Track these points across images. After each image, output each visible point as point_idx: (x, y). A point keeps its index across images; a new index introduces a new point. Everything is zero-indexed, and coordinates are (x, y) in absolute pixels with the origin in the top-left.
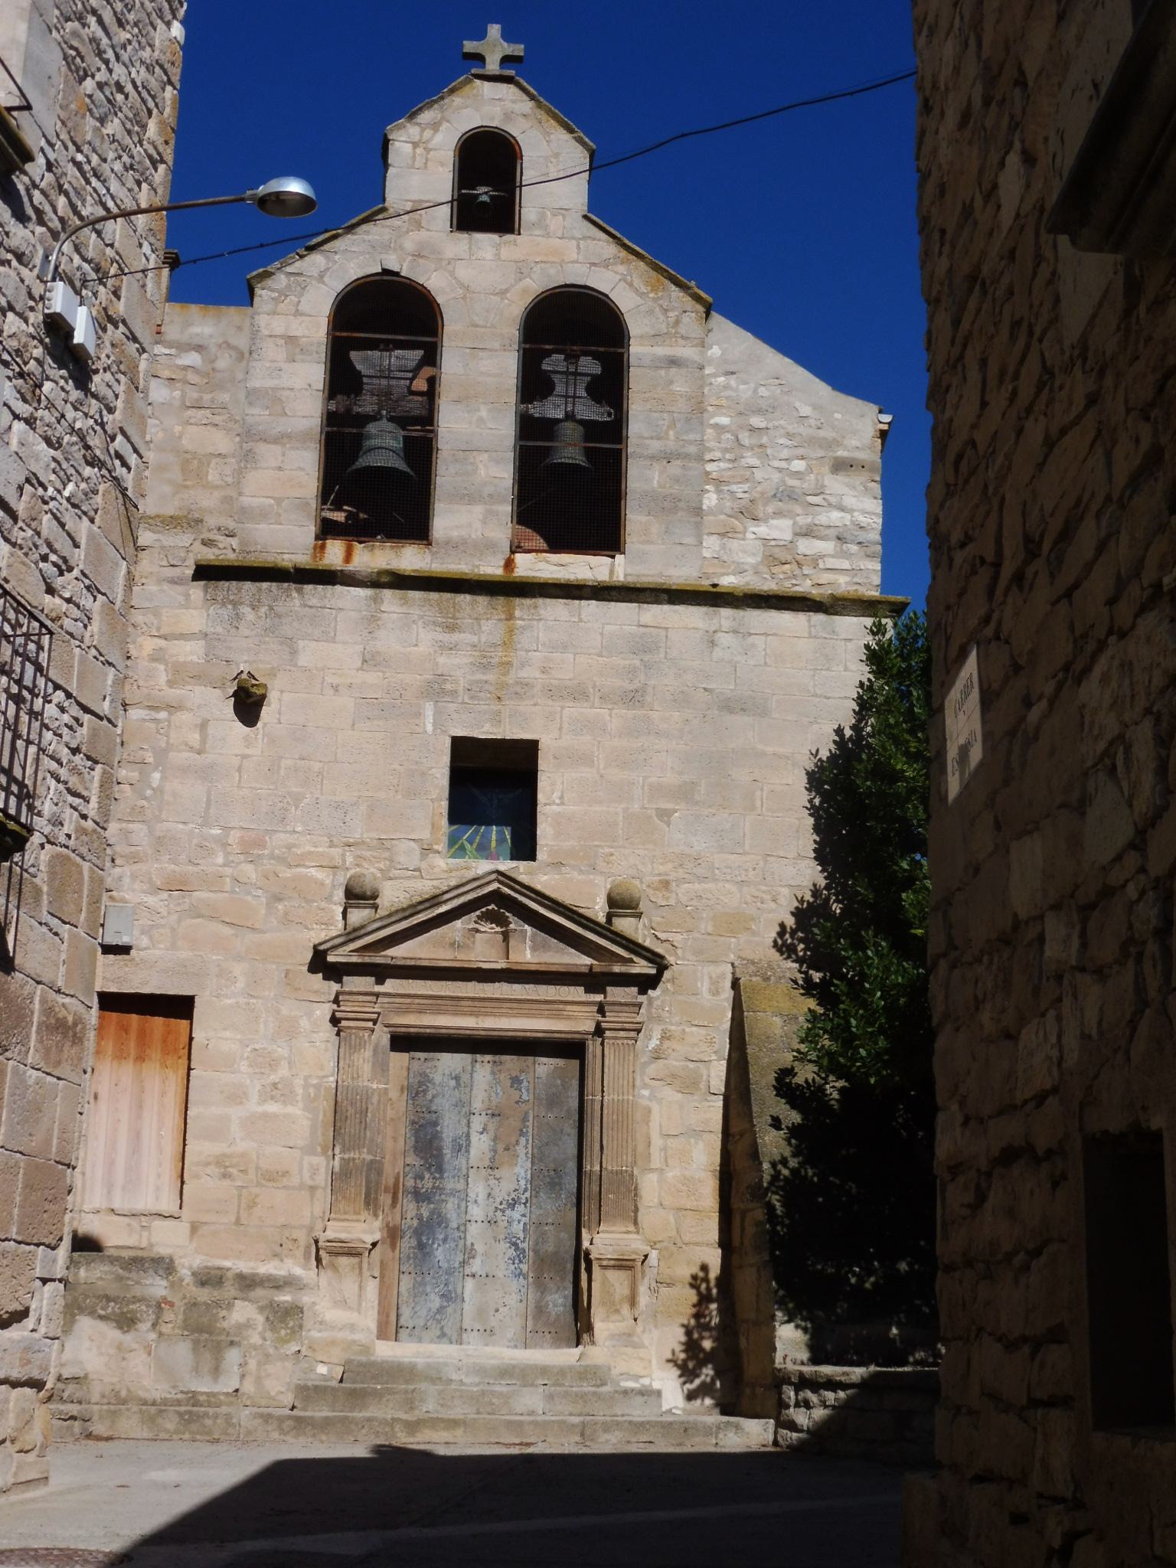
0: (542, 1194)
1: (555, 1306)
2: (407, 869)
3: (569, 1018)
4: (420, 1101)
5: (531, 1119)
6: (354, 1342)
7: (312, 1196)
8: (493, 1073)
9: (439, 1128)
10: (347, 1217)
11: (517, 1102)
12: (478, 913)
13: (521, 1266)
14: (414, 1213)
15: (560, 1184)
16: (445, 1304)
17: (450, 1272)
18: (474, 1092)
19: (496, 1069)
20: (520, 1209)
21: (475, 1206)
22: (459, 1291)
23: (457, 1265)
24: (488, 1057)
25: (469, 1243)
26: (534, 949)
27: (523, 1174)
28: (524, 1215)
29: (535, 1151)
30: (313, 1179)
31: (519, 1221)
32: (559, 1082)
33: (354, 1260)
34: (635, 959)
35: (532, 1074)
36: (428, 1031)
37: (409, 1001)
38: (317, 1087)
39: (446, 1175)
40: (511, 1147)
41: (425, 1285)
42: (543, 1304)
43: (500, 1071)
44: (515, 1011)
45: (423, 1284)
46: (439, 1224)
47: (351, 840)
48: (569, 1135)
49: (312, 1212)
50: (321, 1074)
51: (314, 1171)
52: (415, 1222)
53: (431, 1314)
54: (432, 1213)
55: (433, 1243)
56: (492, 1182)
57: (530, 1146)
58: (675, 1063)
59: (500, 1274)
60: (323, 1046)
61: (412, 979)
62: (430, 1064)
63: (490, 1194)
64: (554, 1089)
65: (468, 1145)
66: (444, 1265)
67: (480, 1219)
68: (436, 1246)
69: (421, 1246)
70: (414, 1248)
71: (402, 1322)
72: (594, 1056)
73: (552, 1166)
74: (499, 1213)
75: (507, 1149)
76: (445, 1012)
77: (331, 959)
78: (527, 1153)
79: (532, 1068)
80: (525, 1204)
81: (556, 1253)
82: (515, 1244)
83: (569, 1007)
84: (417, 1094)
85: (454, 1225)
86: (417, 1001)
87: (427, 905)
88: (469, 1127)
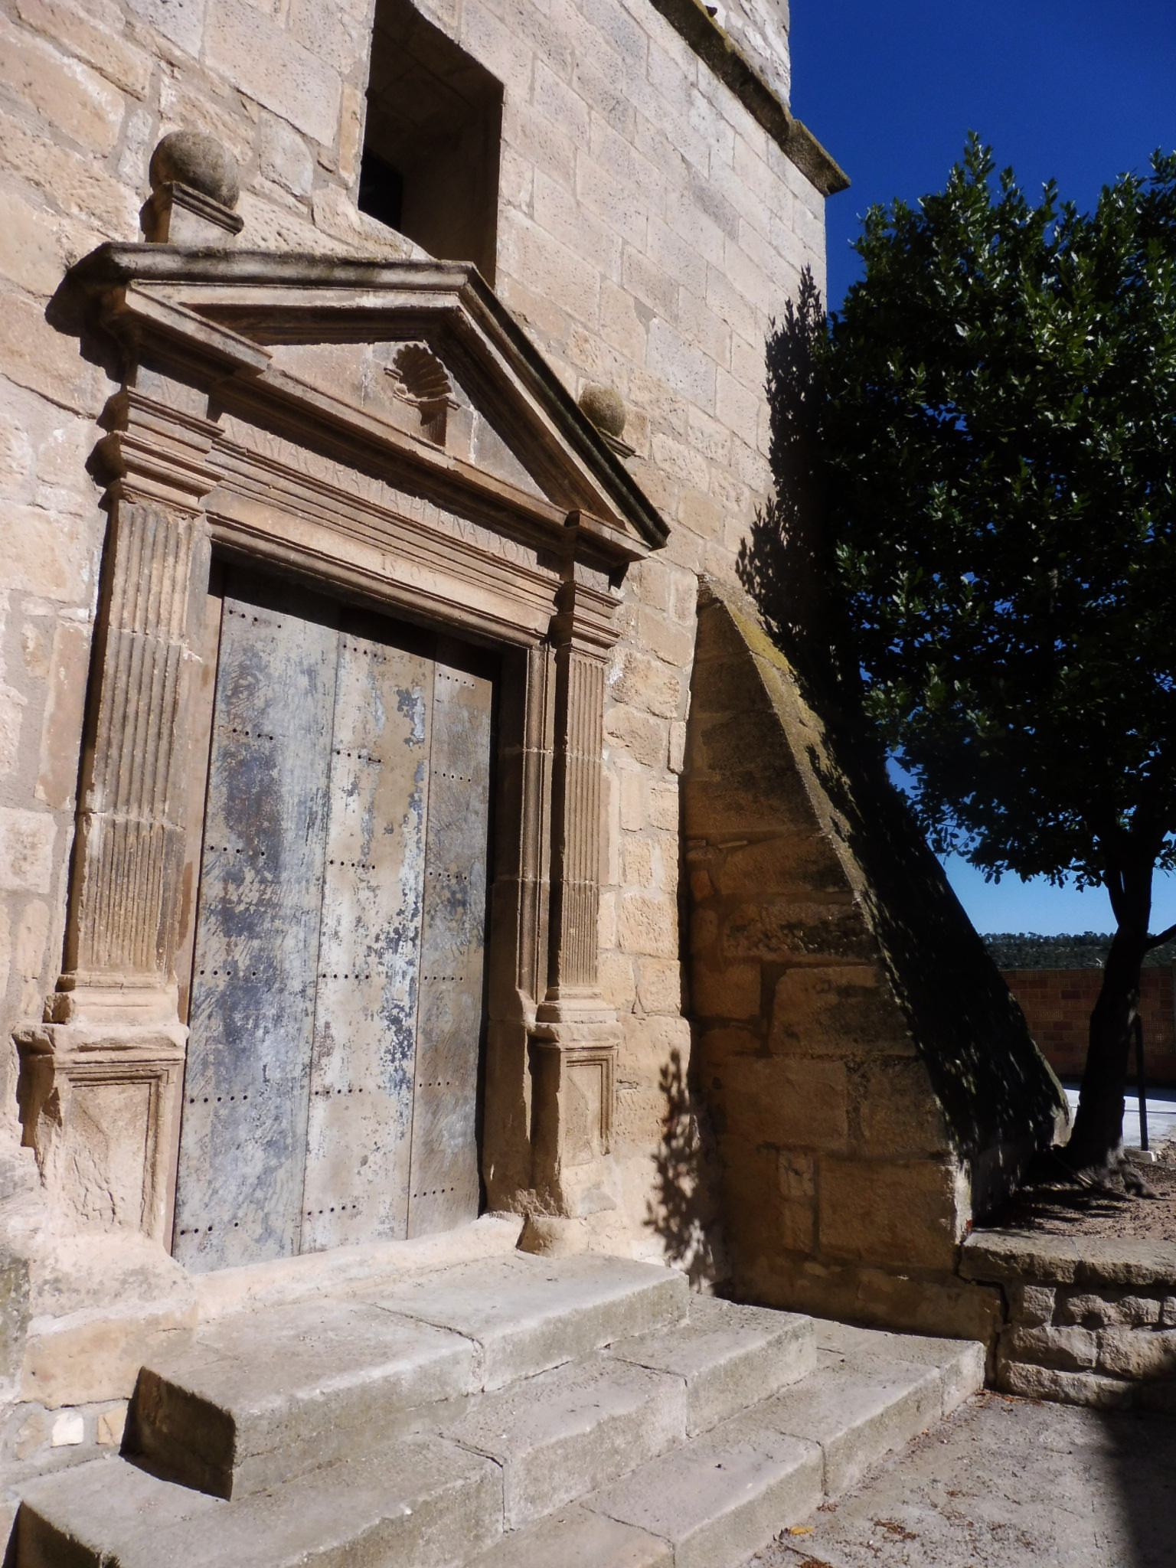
0: (438, 922)
1: (452, 1137)
2: (284, 187)
3: (516, 599)
4: (241, 707)
5: (426, 776)
6: (153, 1322)
7: (16, 917)
8: (372, 676)
9: (275, 773)
10: (119, 977)
11: (407, 741)
12: (401, 345)
13: (405, 1063)
14: (221, 957)
15: (463, 903)
16: (273, 1162)
17: (285, 1090)
18: (339, 707)
19: (377, 669)
20: (406, 947)
21: (334, 945)
22: (300, 1129)
23: (298, 1072)
24: (364, 644)
25: (321, 1023)
26: (481, 452)
27: (412, 882)
28: (411, 963)
29: (431, 837)
30: (18, 871)
31: (404, 974)
32: (466, 714)
33: (139, 1093)
34: (629, 526)
35: (429, 692)
36: (293, 556)
37: (266, 477)
38: (45, 627)
39: (284, 876)
40: (396, 827)
41: (236, 1123)
42: (434, 1135)
43: (383, 675)
44: (445, 562)
45: (231, 1123)
46: (269, 984)
47: (178, 53)
48: (477, 813)
49: (13, 962)
50: (56, 594)
51: (23, 849)
52: (222, 981)
53: (246, 1190)
54: (257, 959)
55: (256, 1026)
56: (365, 894)
57: (423, 827)
58: (635, 711)
59: (370, 1084)
60: (66, 522)
61: (273, 432)
62: (264, 631)
63: (359, 920)
64: (460, 728)
65: (327, 816)
66: (275, 1075)
67: (342, 971)
68: (260, 1033)
69: (231, 1033)
70: (217, 1041)
71: (186, 1219)
72: (545, 678)
73: (454, 869)
74: (373, 959)
75: (390, 830)
76: (333, 526)
77: (133, 301)
78: (418, 842)
79: (429, 679)
80: (413, 940)
81: (455, 1034)
82: (396, 1021)
83: (520, 582)
84: (236, 691)
85: (296, 985)
86: (283, 483)
87: (350, 274)
88: (329, 777)
